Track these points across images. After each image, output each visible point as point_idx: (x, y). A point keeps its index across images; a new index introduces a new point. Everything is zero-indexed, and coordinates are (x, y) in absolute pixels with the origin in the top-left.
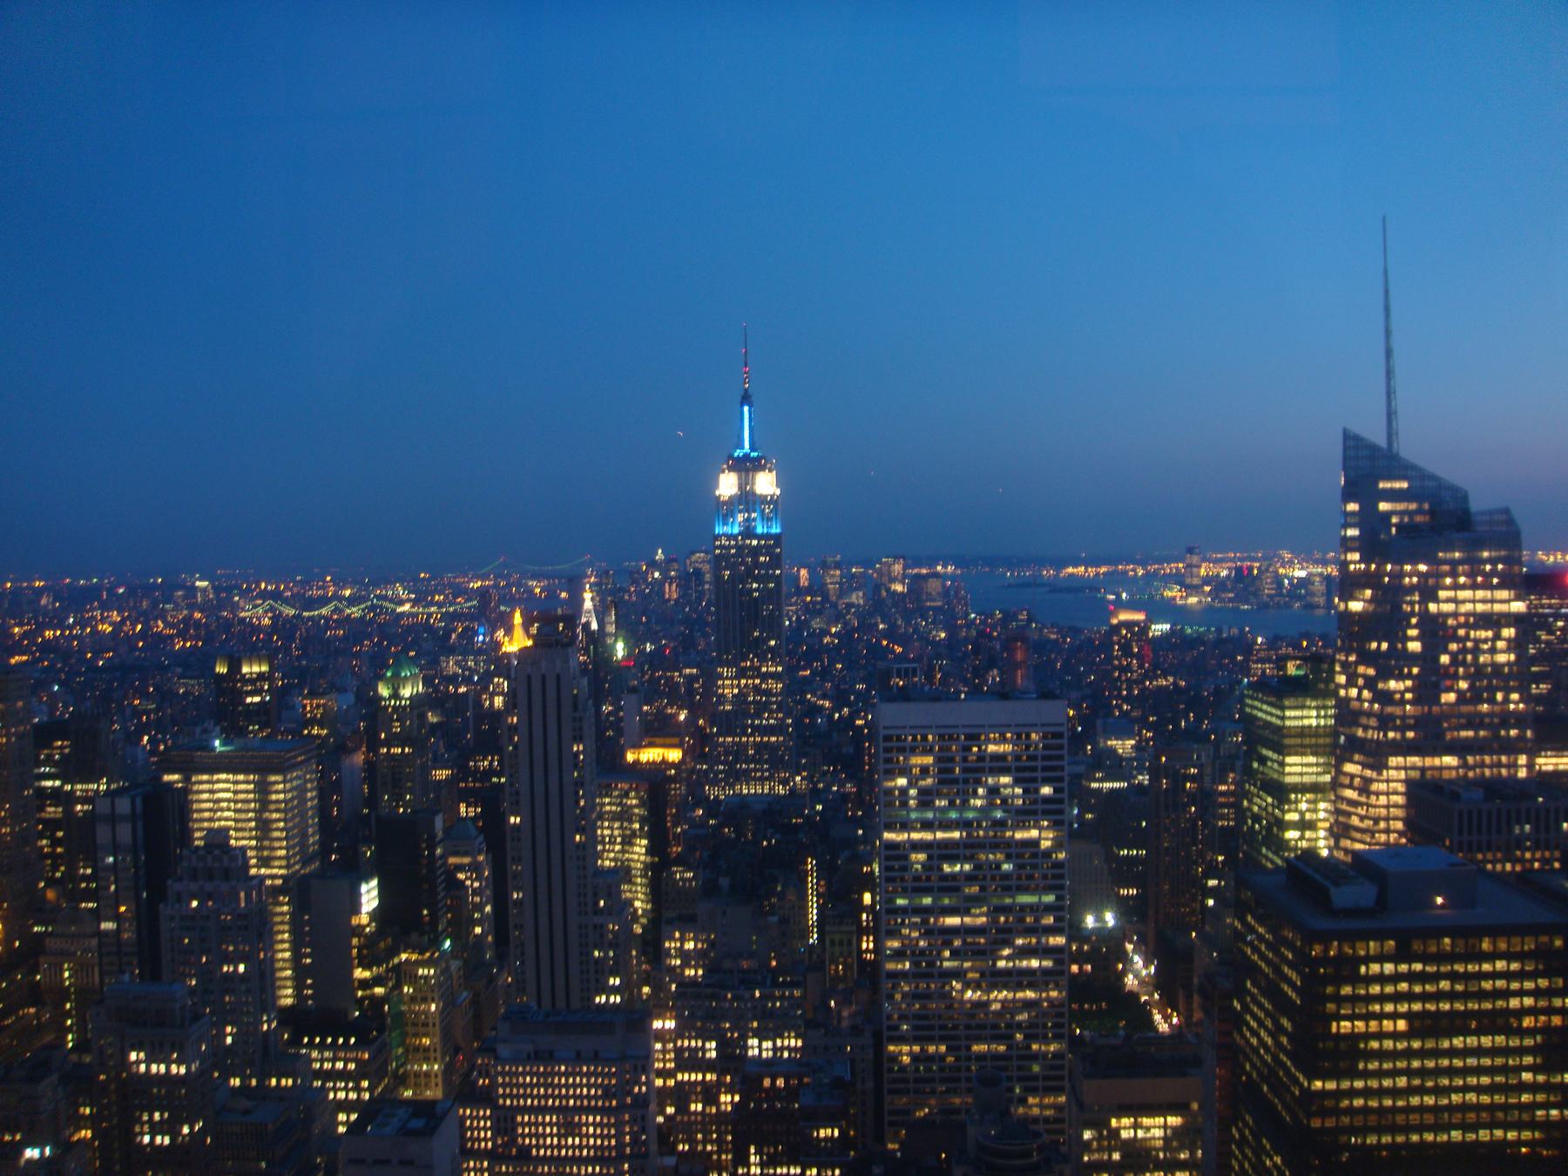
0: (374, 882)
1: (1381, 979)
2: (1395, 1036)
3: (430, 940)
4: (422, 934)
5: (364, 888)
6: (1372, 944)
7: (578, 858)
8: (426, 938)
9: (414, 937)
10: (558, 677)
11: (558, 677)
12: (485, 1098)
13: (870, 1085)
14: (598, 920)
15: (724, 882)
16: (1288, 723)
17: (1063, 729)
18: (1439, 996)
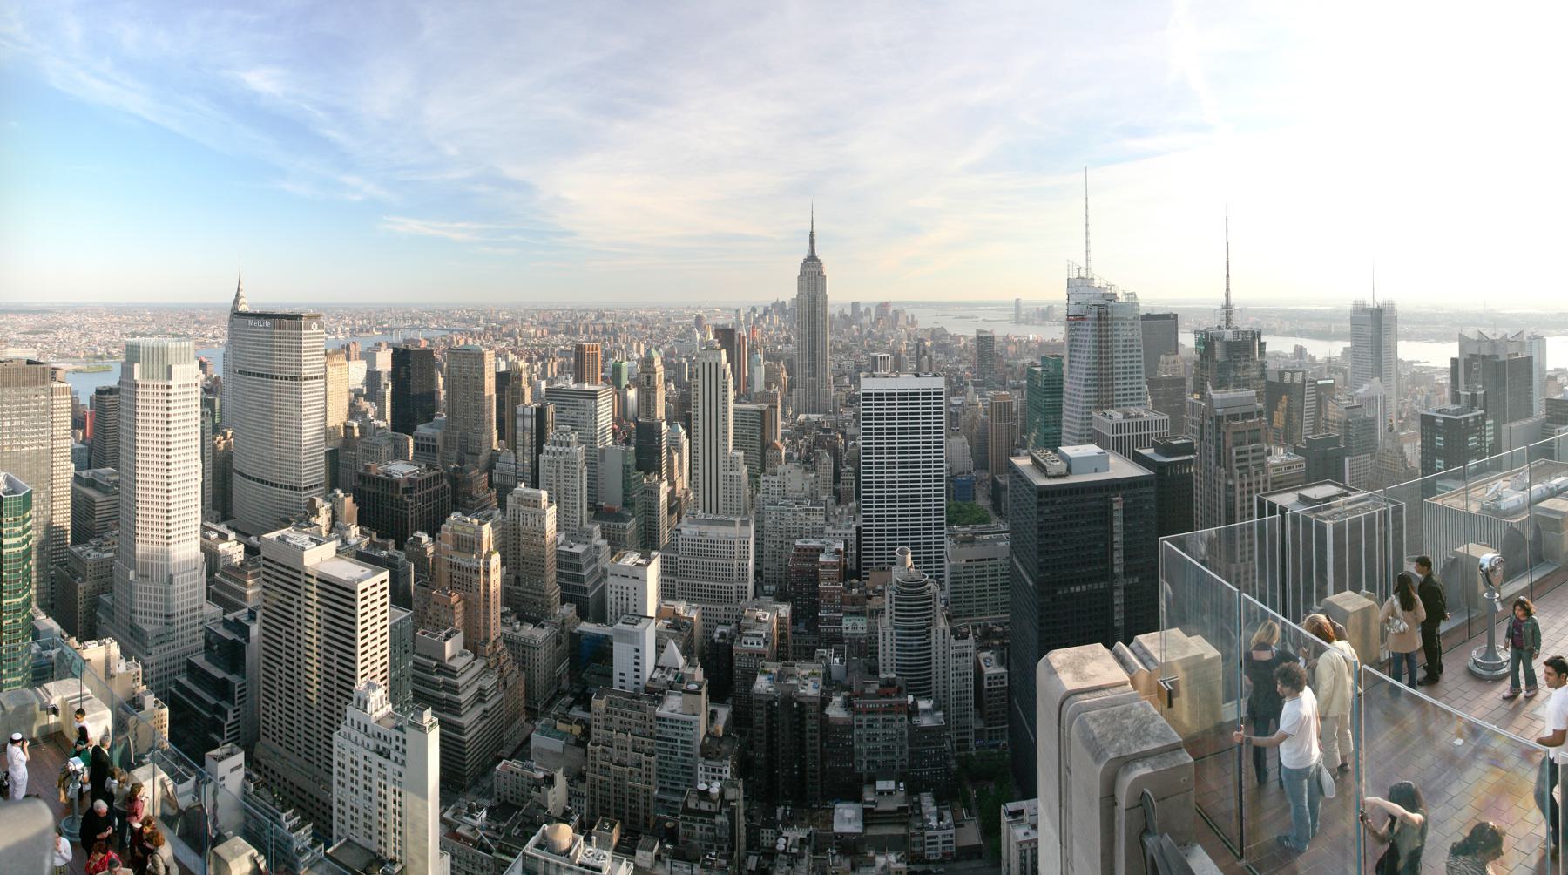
13: (855, 551)
14: (732, 473)
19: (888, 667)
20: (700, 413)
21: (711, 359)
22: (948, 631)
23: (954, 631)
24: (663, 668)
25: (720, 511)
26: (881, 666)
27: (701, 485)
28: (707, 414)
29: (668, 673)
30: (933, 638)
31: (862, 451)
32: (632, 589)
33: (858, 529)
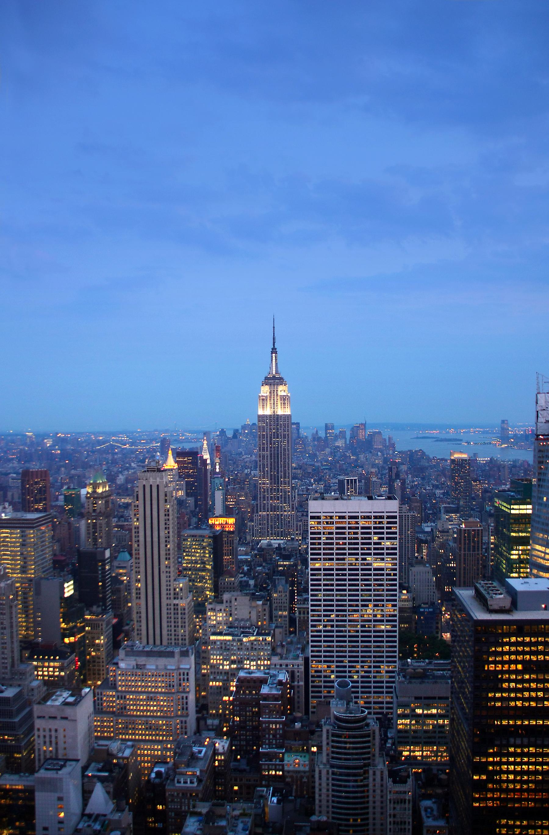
0: (72, 582)
1: (510, 644)
2: (516, 672)
3: (102, 610)
4: (98, 606)
5: (66, 585)
6: (505, 627)
7: (167, 572)
8: (100, 609)
9: (95, 608)
10: (158, 486)
11: (158, 486)
12: (114, 687)
13: (302, 683)
14: (176, 602)
15: (252, 582)
16: (513, 512)
17: (397, 514)
18: (537, 653)
19: (324, 809)
20: (142, 539)
21: (151, 481)
22: (386, 773)
23: (393, 774)
24: (90, 816)
25: (165, 642)
26: (317, 808)
27: (143, 615)
28: (149, 539)
29: (95, 821)
30: (371, 779)
31: (310, 577)
32: (61, 733)
33: (306, 660)
